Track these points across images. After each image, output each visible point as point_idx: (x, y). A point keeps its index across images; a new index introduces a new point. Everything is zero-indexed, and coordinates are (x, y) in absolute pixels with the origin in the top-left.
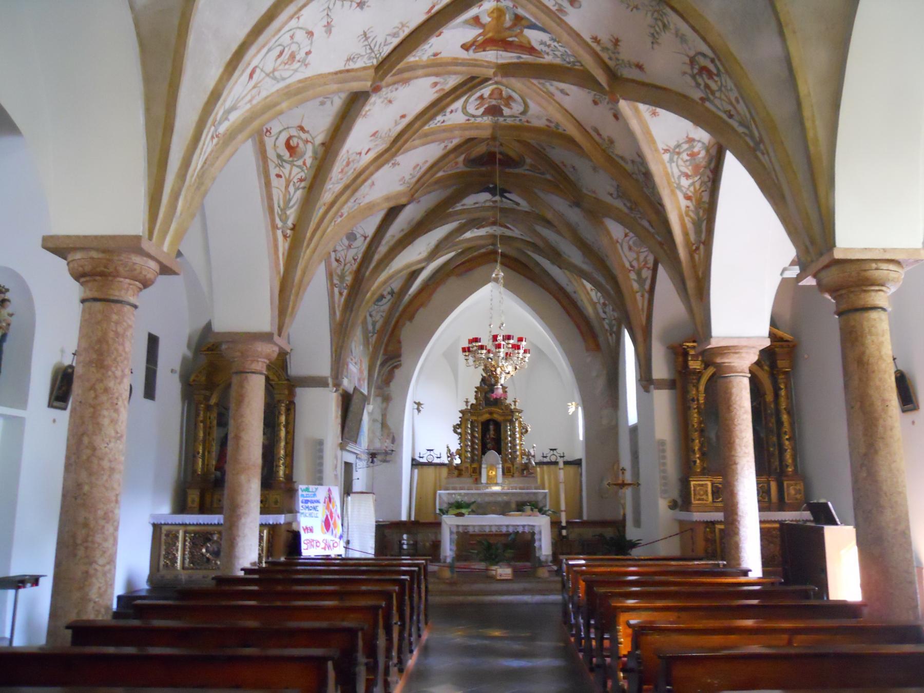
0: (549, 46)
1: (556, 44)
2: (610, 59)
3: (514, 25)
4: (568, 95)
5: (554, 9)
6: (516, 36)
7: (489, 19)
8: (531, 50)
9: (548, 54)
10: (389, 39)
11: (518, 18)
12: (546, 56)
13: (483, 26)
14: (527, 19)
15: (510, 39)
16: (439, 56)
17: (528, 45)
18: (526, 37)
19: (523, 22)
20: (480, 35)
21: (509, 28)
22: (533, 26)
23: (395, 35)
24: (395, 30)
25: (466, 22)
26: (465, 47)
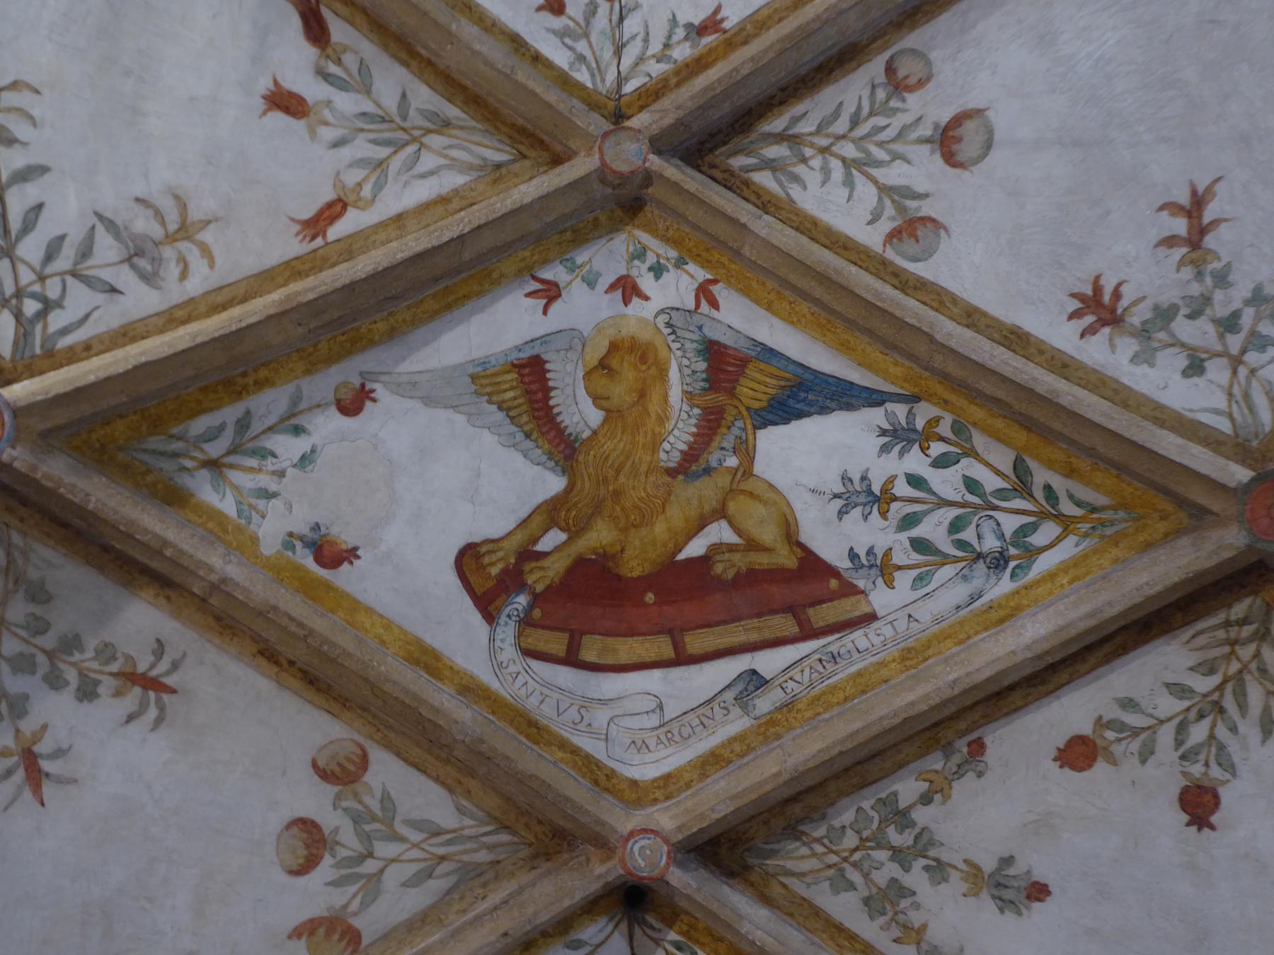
0: (883, 499)
1: (915, 462)
2: (1195, 368)
3: (711, 423)
4: (1039, 892)
5: (872, 237)
6: (720, 513)
7: (595, 416)
8: (800, 590)
9: (886, 569)
10: (107, 249)
11: (722, 365)
12: (881, 598)
13: (563, 448)
14: (770, 353)
15: (695, 548)
16: (344, 577)
17: (786, 559)
18: (772, 497)
19: (755, 388)
20: (551, 512)
21: (691, 464)
22: (801, 396)
23: (138, 253)
24: (143, 224)
25: (483, 380)
26: (488, 576)
